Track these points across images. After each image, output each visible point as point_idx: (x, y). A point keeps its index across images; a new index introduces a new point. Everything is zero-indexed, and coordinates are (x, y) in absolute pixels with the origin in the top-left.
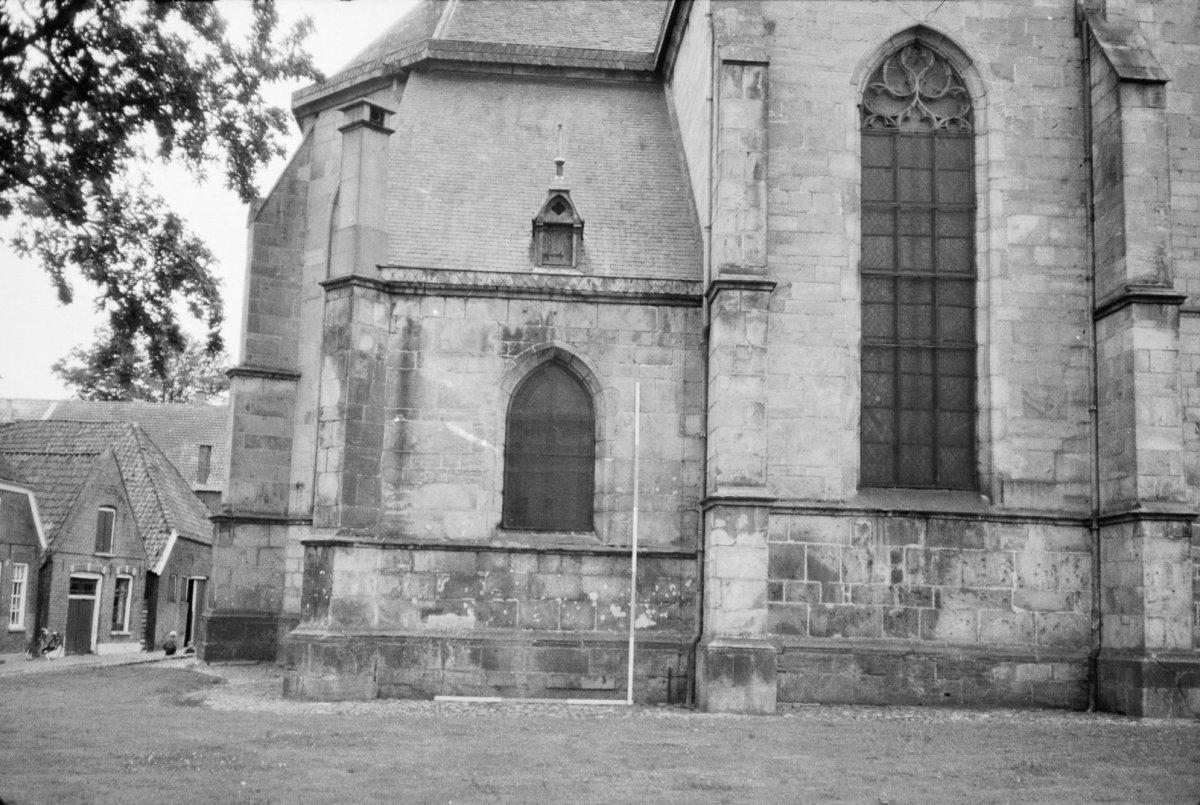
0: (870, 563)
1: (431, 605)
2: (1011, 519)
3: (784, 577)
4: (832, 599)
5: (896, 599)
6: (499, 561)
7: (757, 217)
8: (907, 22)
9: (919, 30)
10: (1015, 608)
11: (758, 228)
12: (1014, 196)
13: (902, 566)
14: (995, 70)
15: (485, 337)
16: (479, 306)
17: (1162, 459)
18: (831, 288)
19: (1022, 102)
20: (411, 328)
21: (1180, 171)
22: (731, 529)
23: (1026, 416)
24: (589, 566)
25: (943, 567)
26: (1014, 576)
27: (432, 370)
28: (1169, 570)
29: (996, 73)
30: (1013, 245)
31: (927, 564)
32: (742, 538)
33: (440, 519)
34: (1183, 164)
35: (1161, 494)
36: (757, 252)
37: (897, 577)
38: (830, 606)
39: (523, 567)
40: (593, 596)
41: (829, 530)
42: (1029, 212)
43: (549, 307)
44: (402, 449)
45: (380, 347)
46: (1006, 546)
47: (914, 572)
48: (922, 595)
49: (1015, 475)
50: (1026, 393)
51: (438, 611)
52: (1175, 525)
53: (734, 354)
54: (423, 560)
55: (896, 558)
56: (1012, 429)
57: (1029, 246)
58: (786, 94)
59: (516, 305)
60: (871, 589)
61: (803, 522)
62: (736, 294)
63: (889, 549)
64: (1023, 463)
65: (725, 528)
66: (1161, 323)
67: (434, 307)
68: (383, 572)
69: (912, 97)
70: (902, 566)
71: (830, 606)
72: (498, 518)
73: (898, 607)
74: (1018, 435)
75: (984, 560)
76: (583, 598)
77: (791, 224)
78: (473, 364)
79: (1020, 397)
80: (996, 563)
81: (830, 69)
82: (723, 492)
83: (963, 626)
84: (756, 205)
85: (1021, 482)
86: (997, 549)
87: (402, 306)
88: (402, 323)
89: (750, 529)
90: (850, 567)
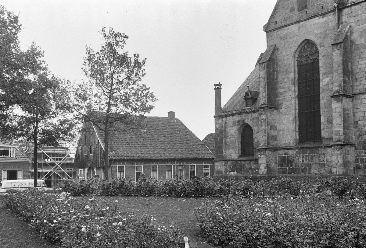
0: (298, 159)
1: (230, 170)
2: (325, 147)
3: (283, 162)
4: (292, 166)
5: (303, 166)
6: (239, 162)
7: (265, 94)
8: (304, 39)
9: (306, 40)
10: (326, 167)
11: (266, 96)
12: (324, 74)
13: (304, 159)
14: (321, 45)
15: (235, 122)
16: (234, 117)
17: (338, 132)
18: (290, 102)
19: (326, 51)
20: (226, 123)
21: (361, 58)
22: (261, 155)
23: (328, 124)
24: (252, 162)
25: (312, 159)
26: (326, 159)
27: (229, 129)
28: (337, 157)
29: (321, 46)
30: (324, 85)
31: (308, 158)
32: (262, 156)
33: (231, 155)
34: (362, 56)
35: (338, 140)
36: (266, 100)
37: (303, 161)
38: (291, 168)
39: (243, 163)
40: (253, 168)
41: (291, 152)
42: (328, 77)
43: (244, 115)
44: (226, 143)
45: (221, 127)
46: (324, 153)
47: (306, 160)
48: (307, 165)
49: (326, 137)
50: (327, 118)
51: (232, 171)
52: (339, 147)
53: (261, 121)
54: (229, 163)
55: (303, 157)
56: (325, 127)
57: (327, 85)
58: (281, 63)
59: (239, 116)
60: (298, 164)
61: (286, 151)
62: (261, 110)
63: (301, 155)
64: (328, 134)
65: (260, 155)
66: (338, 102)
67: (228, 118)
68: (224, 165)
69: (307, 55)
70: (304, 159)
71: (291, 168)
72: (240, 154)
73: (303, 167)
74: (326, 128)
75: (319, 156)
76: (251, 168)
77: (282, 90)
78: (234, 128)
79: (326, 120)
80: (322, 157)
81: (289, 55)
82: (259, 148)
83: (316, 171)
84: (265, 91)
85: (327, 139)
86: (322, 154)
87: (224, 119)
88: (224, 122)
89: (263, 154)
90: (295, 159)
